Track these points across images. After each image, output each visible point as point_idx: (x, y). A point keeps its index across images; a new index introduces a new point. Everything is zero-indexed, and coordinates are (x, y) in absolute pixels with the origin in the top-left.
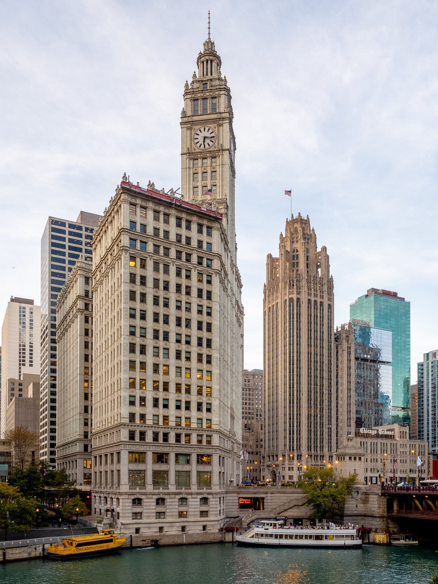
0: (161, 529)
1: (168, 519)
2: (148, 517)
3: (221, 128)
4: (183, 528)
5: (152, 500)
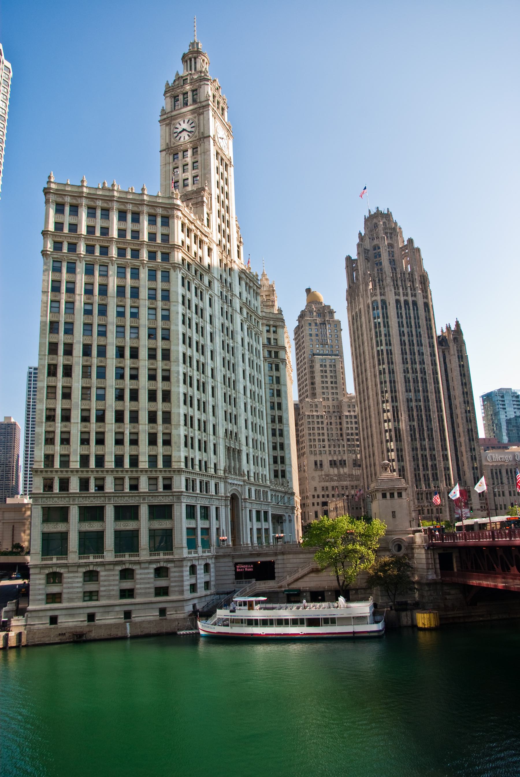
2: (71, 600)
3: (202, 117)
4: (128, 615)
5: (76, 575)
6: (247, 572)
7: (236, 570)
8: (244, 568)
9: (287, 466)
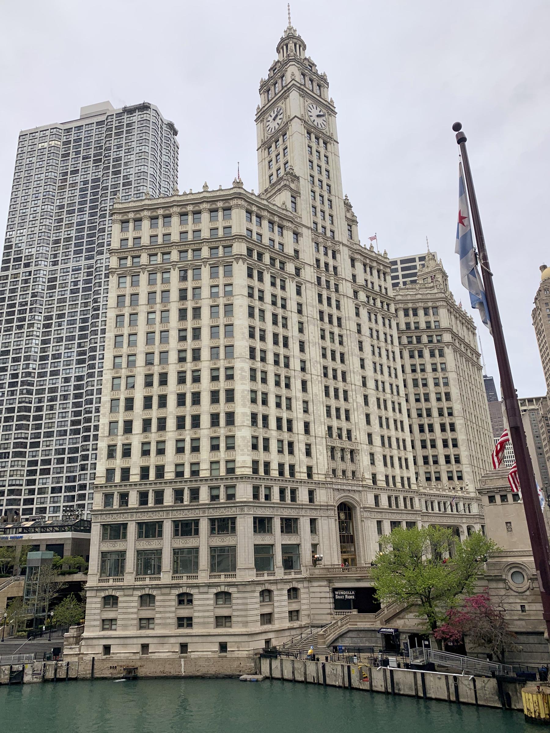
0: (145, 647)
1: (158, 631)
2: (125, 627)
3: (288, 100)
4: (184, 647)
6: (348, 599)
7: (334, 597)
8: (344, 595)
9: (464, 466)
